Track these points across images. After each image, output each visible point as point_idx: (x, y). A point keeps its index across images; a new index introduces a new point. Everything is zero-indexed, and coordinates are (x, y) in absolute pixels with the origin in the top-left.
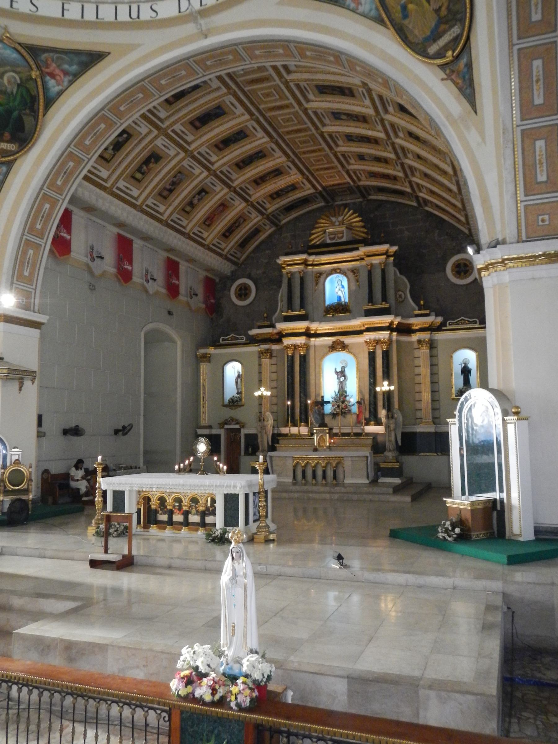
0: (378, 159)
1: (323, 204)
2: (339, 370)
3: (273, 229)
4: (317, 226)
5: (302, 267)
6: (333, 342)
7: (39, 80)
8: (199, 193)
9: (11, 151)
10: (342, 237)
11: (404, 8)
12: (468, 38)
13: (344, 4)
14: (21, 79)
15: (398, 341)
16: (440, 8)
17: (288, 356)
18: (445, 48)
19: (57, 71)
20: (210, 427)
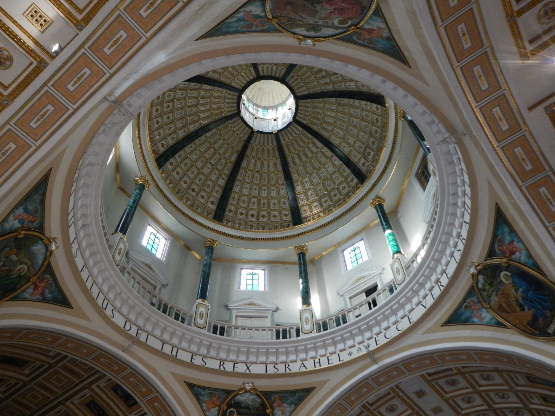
7: (30, 283)
13: (201, 404)
14: (26, 274)
19: (40, 289)
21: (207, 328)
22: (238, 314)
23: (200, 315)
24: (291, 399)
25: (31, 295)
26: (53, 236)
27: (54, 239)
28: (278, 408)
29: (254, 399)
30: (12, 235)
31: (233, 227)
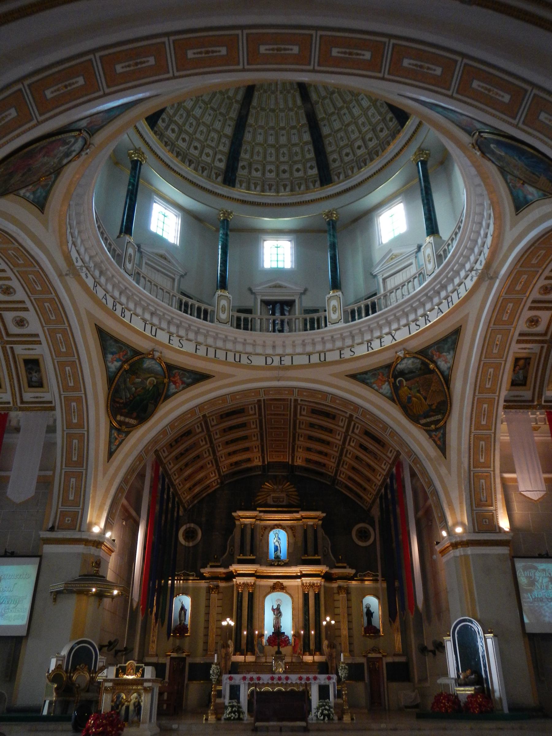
0: (320, 453)
1: (260, 473)
2: (275, 607)
3: (218, 486)
4: (261, 490)
6: (275, 584)
7: (166, 385)
8: (194, 458)
9: (133, 424)
10: (283, 501)
11: (410, 398)
12: (446, 422)
14: (157, 382)
15: (325, 586)
16: (432, 405)
17: (238, 593)
18: (431, 423)
20: (157, 655)
21: (342, 320)
22: (385, 276)
23: (333, 310)
24: (446, 347)
25: (176, 388)
26: (150, 349)
27: (153, 350)
28: (440, 360)
29: (413, 362)
30: (121, 371)
31: (347, 177)
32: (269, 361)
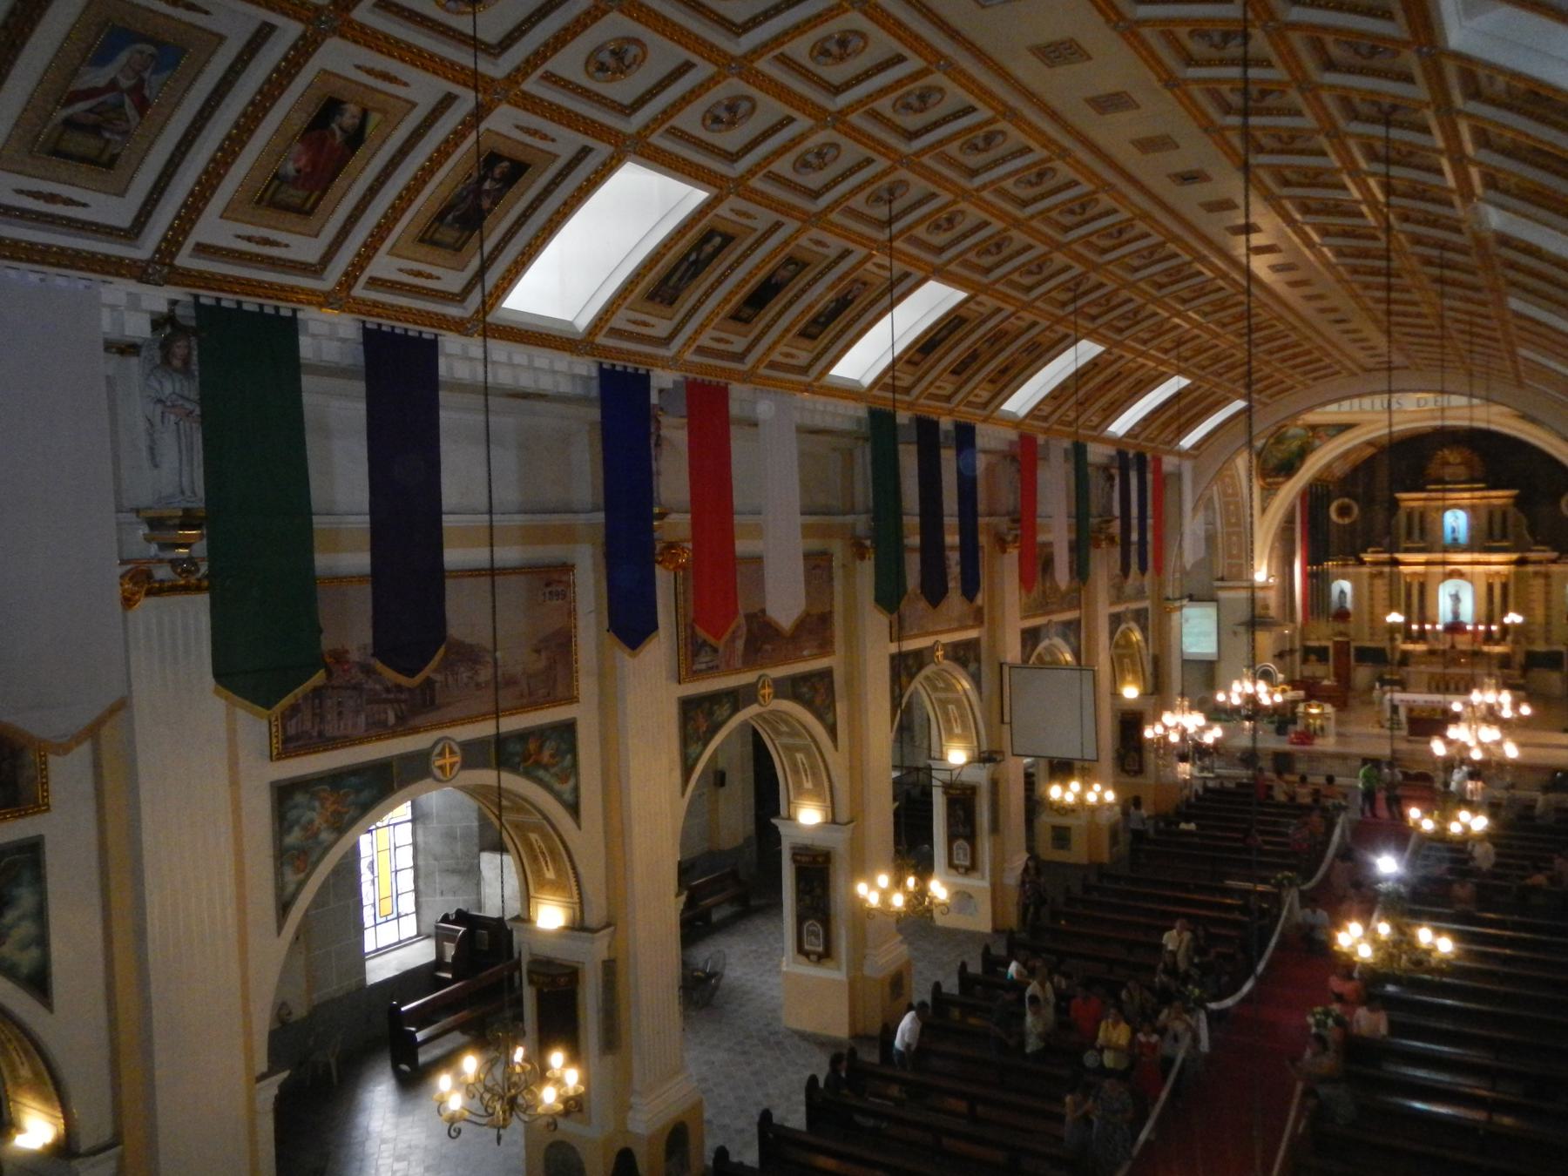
5: (1421, 503)
32: (1422, 402)
